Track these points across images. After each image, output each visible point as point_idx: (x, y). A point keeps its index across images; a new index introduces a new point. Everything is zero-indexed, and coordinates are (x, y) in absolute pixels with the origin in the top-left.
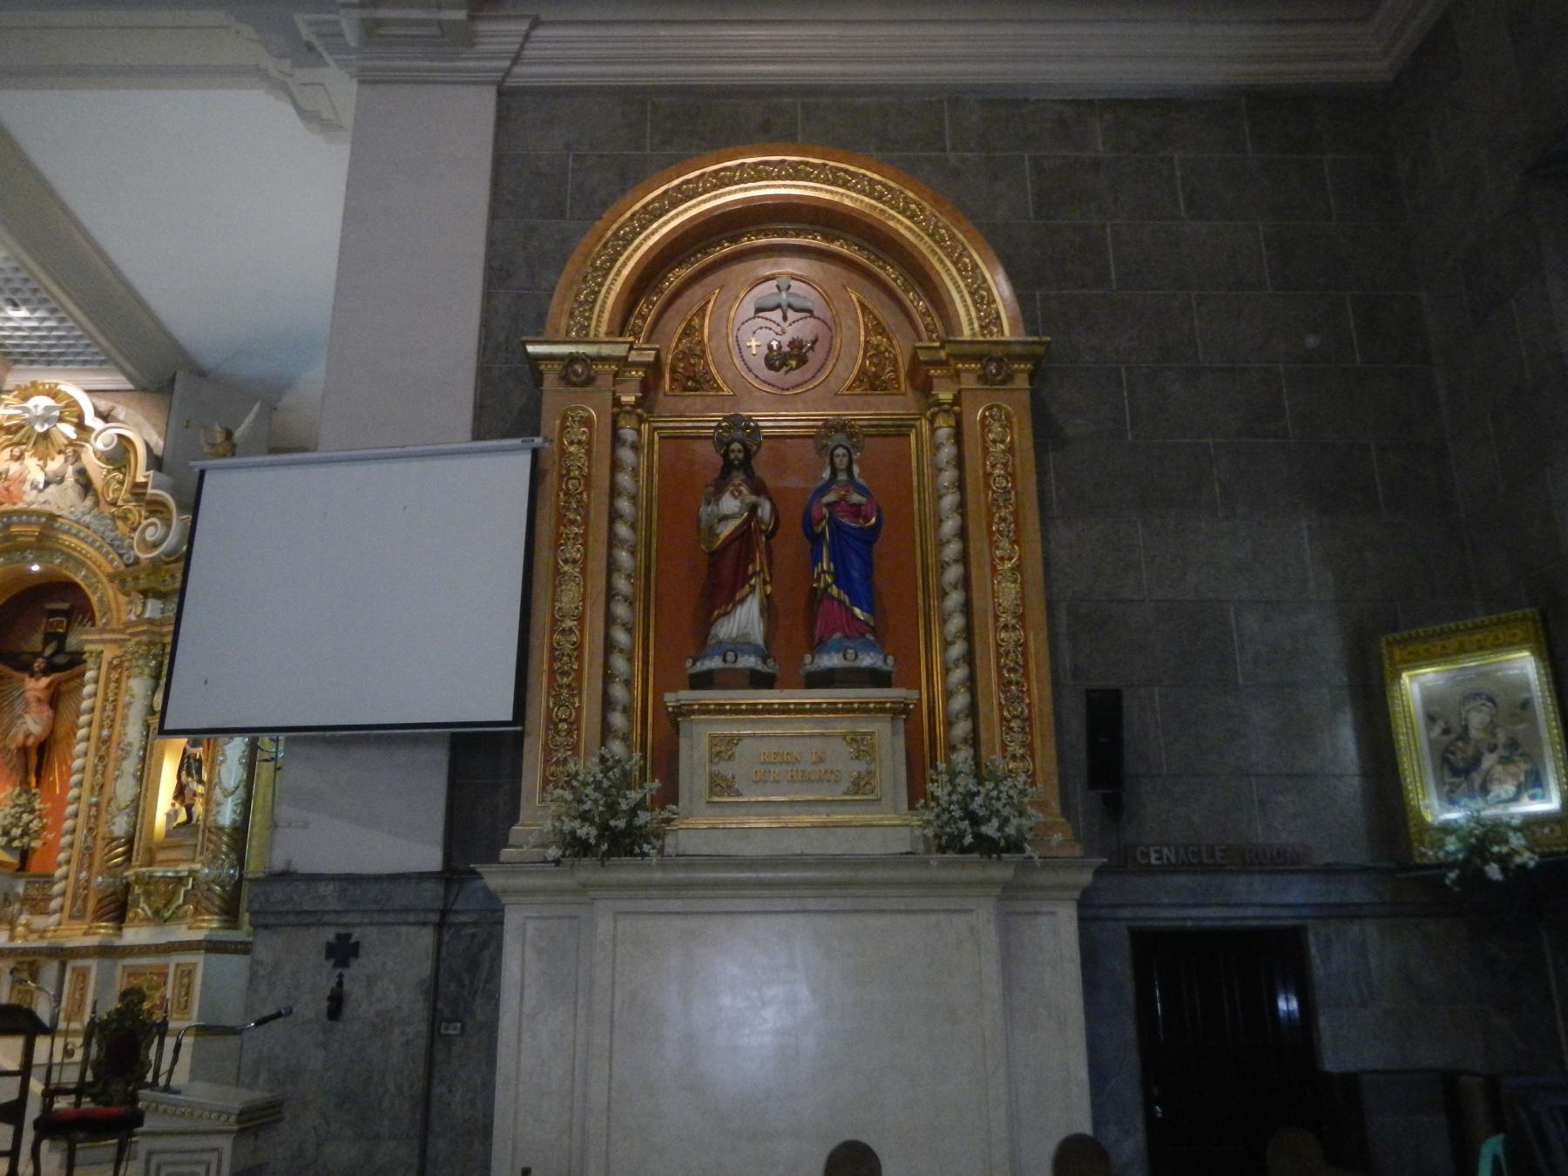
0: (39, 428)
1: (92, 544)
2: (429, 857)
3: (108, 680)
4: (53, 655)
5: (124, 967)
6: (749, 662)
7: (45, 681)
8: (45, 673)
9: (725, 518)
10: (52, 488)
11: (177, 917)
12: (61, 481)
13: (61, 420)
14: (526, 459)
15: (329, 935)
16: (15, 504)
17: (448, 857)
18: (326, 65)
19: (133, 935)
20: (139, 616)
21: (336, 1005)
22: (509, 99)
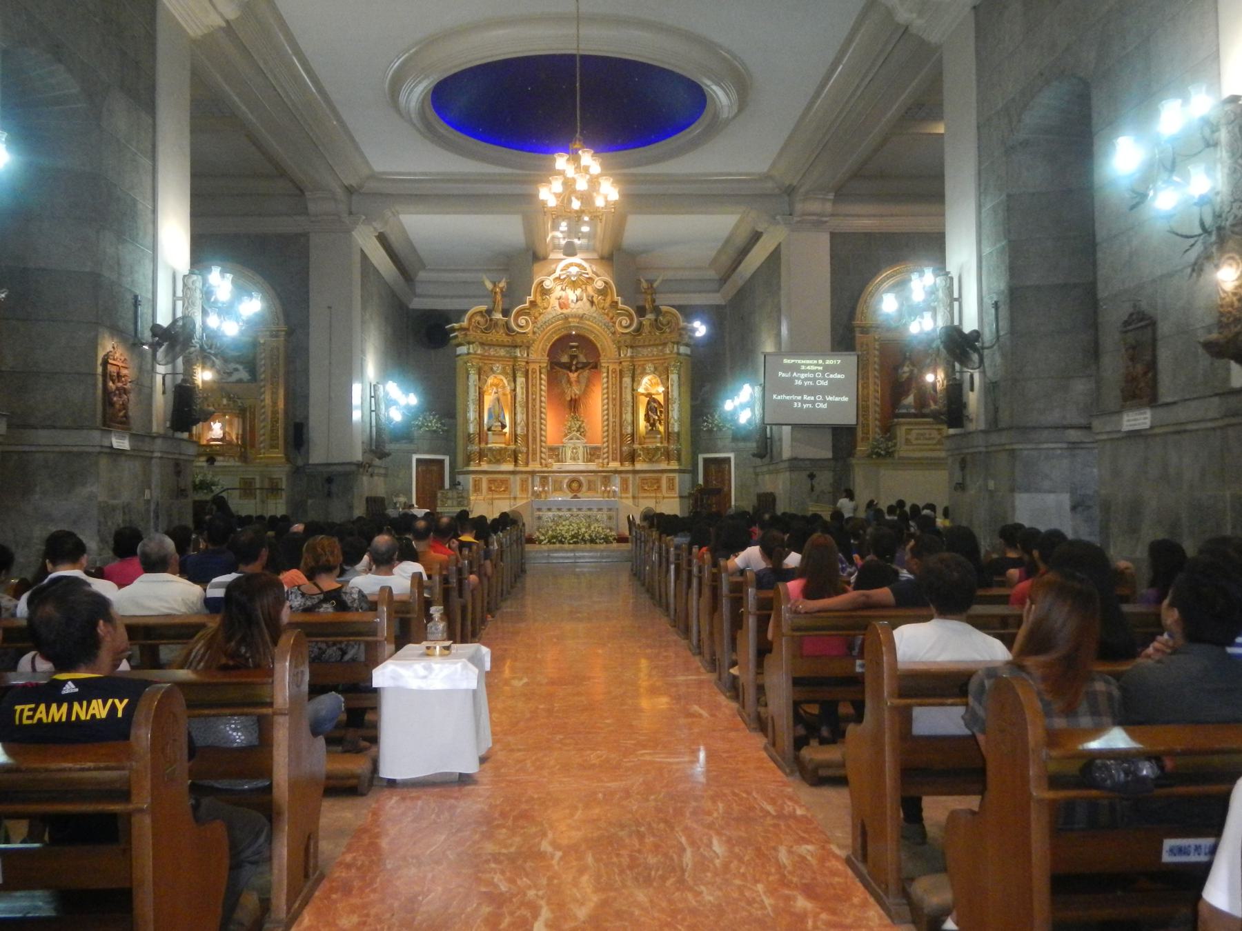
0: (573, 279)
1: (598, 325)
2: (829, 455)
4: (577, 363)
6: (913, 411)
7: (576, 374)
8: (576, 371)
9: (904, 373)
11: (658, 461)
13: (581, 275)
14: (855, 358)
15: (808, 473)
17: (833, 455)
18: (778, 223)
19: (639, 466)
20: (625, 355)
21: (812, 489)
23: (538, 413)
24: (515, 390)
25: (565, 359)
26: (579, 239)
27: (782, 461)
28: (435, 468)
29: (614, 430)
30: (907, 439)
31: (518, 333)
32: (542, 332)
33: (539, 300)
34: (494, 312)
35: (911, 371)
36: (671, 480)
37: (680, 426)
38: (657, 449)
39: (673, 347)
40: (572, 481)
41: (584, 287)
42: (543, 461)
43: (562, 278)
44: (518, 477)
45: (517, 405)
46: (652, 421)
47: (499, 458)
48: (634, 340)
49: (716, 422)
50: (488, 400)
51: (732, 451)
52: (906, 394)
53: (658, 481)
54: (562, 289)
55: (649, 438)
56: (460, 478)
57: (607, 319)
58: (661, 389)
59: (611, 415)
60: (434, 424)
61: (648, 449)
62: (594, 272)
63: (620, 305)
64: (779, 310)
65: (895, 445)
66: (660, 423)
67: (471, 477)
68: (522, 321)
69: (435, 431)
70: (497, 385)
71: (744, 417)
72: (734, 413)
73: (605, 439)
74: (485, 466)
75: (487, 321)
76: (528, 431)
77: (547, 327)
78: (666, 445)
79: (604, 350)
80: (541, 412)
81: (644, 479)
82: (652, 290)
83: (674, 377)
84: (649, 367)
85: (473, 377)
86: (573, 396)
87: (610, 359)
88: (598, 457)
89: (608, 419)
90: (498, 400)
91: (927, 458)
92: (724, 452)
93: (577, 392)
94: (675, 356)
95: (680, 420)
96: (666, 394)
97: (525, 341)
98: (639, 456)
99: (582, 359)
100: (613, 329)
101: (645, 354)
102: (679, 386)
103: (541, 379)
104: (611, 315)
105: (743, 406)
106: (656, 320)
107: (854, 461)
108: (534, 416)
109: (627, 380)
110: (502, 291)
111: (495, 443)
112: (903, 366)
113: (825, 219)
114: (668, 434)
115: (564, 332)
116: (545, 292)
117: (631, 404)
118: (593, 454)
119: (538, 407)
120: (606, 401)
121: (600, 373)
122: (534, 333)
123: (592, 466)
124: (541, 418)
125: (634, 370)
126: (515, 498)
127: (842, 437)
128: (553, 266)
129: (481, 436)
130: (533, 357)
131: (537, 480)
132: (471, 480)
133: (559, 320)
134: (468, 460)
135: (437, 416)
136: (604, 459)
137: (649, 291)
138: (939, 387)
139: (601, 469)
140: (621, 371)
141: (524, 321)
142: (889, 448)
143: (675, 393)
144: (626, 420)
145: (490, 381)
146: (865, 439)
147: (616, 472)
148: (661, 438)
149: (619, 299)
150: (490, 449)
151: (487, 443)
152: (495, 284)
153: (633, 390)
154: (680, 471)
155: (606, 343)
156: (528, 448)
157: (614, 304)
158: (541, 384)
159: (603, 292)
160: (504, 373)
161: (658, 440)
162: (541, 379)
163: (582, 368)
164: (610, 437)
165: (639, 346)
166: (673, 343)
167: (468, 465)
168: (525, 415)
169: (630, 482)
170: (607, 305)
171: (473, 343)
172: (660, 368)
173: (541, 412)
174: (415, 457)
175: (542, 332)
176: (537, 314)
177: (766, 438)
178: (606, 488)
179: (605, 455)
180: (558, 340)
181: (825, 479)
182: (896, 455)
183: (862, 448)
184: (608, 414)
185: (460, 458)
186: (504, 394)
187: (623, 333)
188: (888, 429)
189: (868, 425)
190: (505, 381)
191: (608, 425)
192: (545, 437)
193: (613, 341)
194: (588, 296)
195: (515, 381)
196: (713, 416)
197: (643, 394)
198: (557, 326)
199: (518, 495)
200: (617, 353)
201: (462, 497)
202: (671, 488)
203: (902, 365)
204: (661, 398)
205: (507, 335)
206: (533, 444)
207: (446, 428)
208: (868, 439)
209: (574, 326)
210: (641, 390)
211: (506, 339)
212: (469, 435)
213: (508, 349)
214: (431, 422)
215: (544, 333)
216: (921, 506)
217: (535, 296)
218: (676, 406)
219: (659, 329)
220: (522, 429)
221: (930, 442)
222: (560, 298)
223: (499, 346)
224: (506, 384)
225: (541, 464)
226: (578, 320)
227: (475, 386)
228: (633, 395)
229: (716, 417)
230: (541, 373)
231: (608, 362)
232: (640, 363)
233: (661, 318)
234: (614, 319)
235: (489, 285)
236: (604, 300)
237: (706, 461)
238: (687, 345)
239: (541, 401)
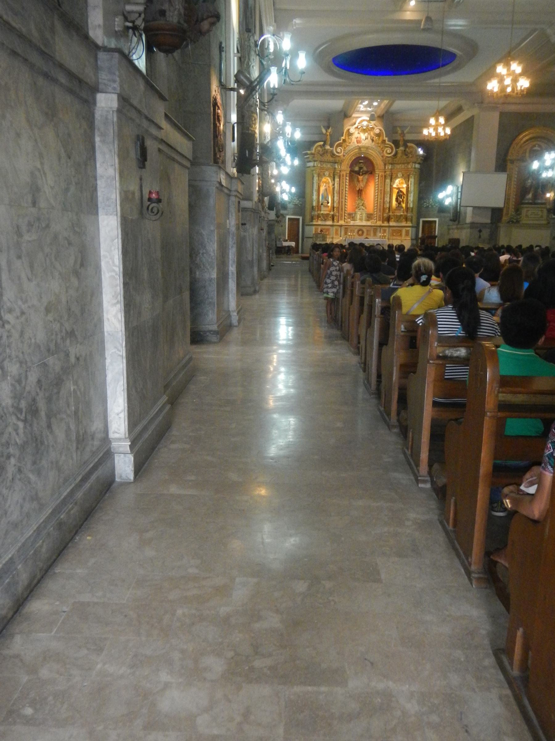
0: (364, 128)
1: (375, 152)
3: (381, 179)
4: (362, 172)
5: (392, 229)
6: (531, 201)
7: (362, 177)
8: (362, 175)
10: (366, 140)
11: (401, 222)
12: (367, 139)
15: (479, 229)
16: (360, 143)
19: (392, 224)
20: (388, 168)
21: (480, 237)
22: (502, 114)
23: (344, 196)
24: (334, 185)
25: (357, 169)
26: (370, 108)
27: (466, 224)
28: (295, 222)
29: (380, 206)
30: (526, 215)
31: (337, 156)
32: (347, 155)
33: (347, 139)
34: (326, 145)
35: (532, 182)
36: (407, 232)
37: (413, 204)
38: (401, 215)
39: (413, 165)
40: (359, 231)
41: (369, 132)
42: (345, 220)
43: (359, 127)
44: (334, 228)
45: (335, 192)
46: (399, 202)
47: (326, 218)
48: (393, 160)
49: (431, 203)
50: (322, 189)
51: (437, 217)
52: (529, 193)
53: (401, 231)
54: (358, 133)
55: (397, 210)
56: (307, 228)
57: (379, 149)
58: (405, 186)
59: (379, 198)
60: (297, 202)
61: (397, 215)
62: (375, 125)
63: (387, 142)
64: (471, 150)
65: (521, 217)
66: (403, 203)
67: (314, 227)
68: (339, 150)
69: (296, 205)
70: (325, 182)
71: (447, 202)
72: (443, 199)
73: (376, 210)
74: (320, 222)
75: (323, 150)
76: (339, 205)
77: (350, 153)
78: (406, 213)
79: (377, 165)
80: (345, 196)
81: (393, 230)
82: (403, 134)
83: (412, 180)
84: (400, 175)
85: (316, 178)
86: (360, 189)
87: (380, 170)
88: (372, 219)
89: (377, 200)
90: (326, 190)
91: (536, 224)
92: (433, 218)
93: (362, 186)
94: (413, 169)
95: (413, 201)
96: (407, 188)
97: (340, 160)
98: (392, 219)
99: (365, 169)
100: (382, 155)
101: (398, 168)
102: (414, 184)
103: (346, 179)
104: (381, 147)
105: (447, 196)
106: (405, 151)
107: (500, 225)
108: (342, 198)
109: (388, 181)
110: (330, 135)
111: (324, 211)
112: (528, 179)
113: (498, 106)
114: (407, 208)
115: (358, 155)
116: (350, 134)
117: (389, 193)
118: (369, 217)
119: (344, 193)
120: (377, 191)
121: (374, 177)
122: (344, 156)
123: (369, 223)
124: (345, 199)
125: (392, 175)
126: (333, 238)
127: (496, 213)
128: (354, 121)
129: (319, 208)
130: (343, 168)
131: (343, 228)
132: (314, 228)
133: (356, 149)
134: (312, 219)
135: (297, 197)
136: (374, 220)
137: (402, 135)
138: (551, 199)
139: (373, 225)
140: (385, 176)
141: (340, 150)
142: (518, 219)
143: (412, 188)
144: (386, 201)
145: (324, 180)
146: (507, 214)
147: (381, 226)
148: (403, 210)
149: (386, 139)
150: (322, 214)
151: (321, 211)
152: (327, 131)
153: (391, 186)
154: (412, 227)
155: (378, 162)
156: (339, 213)
157: (384, 141)
158: (346, 182)
159: (378, 135)
160: (329, 176)
161: (402, 211)
162: (346, 179)
163: (365, 174)
164: (378, 208)
165: (396, 164)
166: (413, 163)
167: (312, 221)
168: (338, 198)
169: (387, 231)
170: (380, 142)
171: (317, 161)
172: (405, 175)
173: (345, 196)
174: (287, 217)
175: (347, 155)
176: (345, 146)
177: (457, 212)
178: (353, 234)
179: (375, 218)
180: (355, 160)
181: (486, 233)
182: (521, 223)
183: (505, 218)
184: (377, 198)
185: (308, 217)
186: (329, 187)
187: (387, 157)
188: (517, 210)
189: (509, 208)
190: (330, 180)
191: (377, 203)
192: (347, 208)
193: (382, 160)
194: (371, 137)
195: (334, 180)
196: (429, 200)
197: (395, 188)
198: (356, 152)
199: (334, 237)
200: (383, 167)
201: (324, 237)
202: (407, 233)
203: (528, 178)
204: (404, 190)
205: (332, 157)
206: (341, 211)
207: (301, 203)
208: (508, 214)
209: (363, 153)
210: (395, 186)
211: (331, 159)
212: (313, 207)
213: (332, 164)
214: (295, 200)
215: (349, 156)
216: (534, 246)
217: (345, 137)
218: (412, 195)
219: (406, 155)
220: (337, 204)
221: (536, 216)
222: (357, 138)
223: (328, 162)
224: (330, 182)
225: (344, 221)
226: (365, 149)
227: (317, 183)
228: (391, 189)
229: (431, 200)
230: (346, 176)
231: (379, 172)
232: (395, 172)
233: (407, 149)
234: (383, 149)
235: (324, 131)
236: (379, 139)
237: (424, 222)
238: (419, 163)
239: (346, 191)
